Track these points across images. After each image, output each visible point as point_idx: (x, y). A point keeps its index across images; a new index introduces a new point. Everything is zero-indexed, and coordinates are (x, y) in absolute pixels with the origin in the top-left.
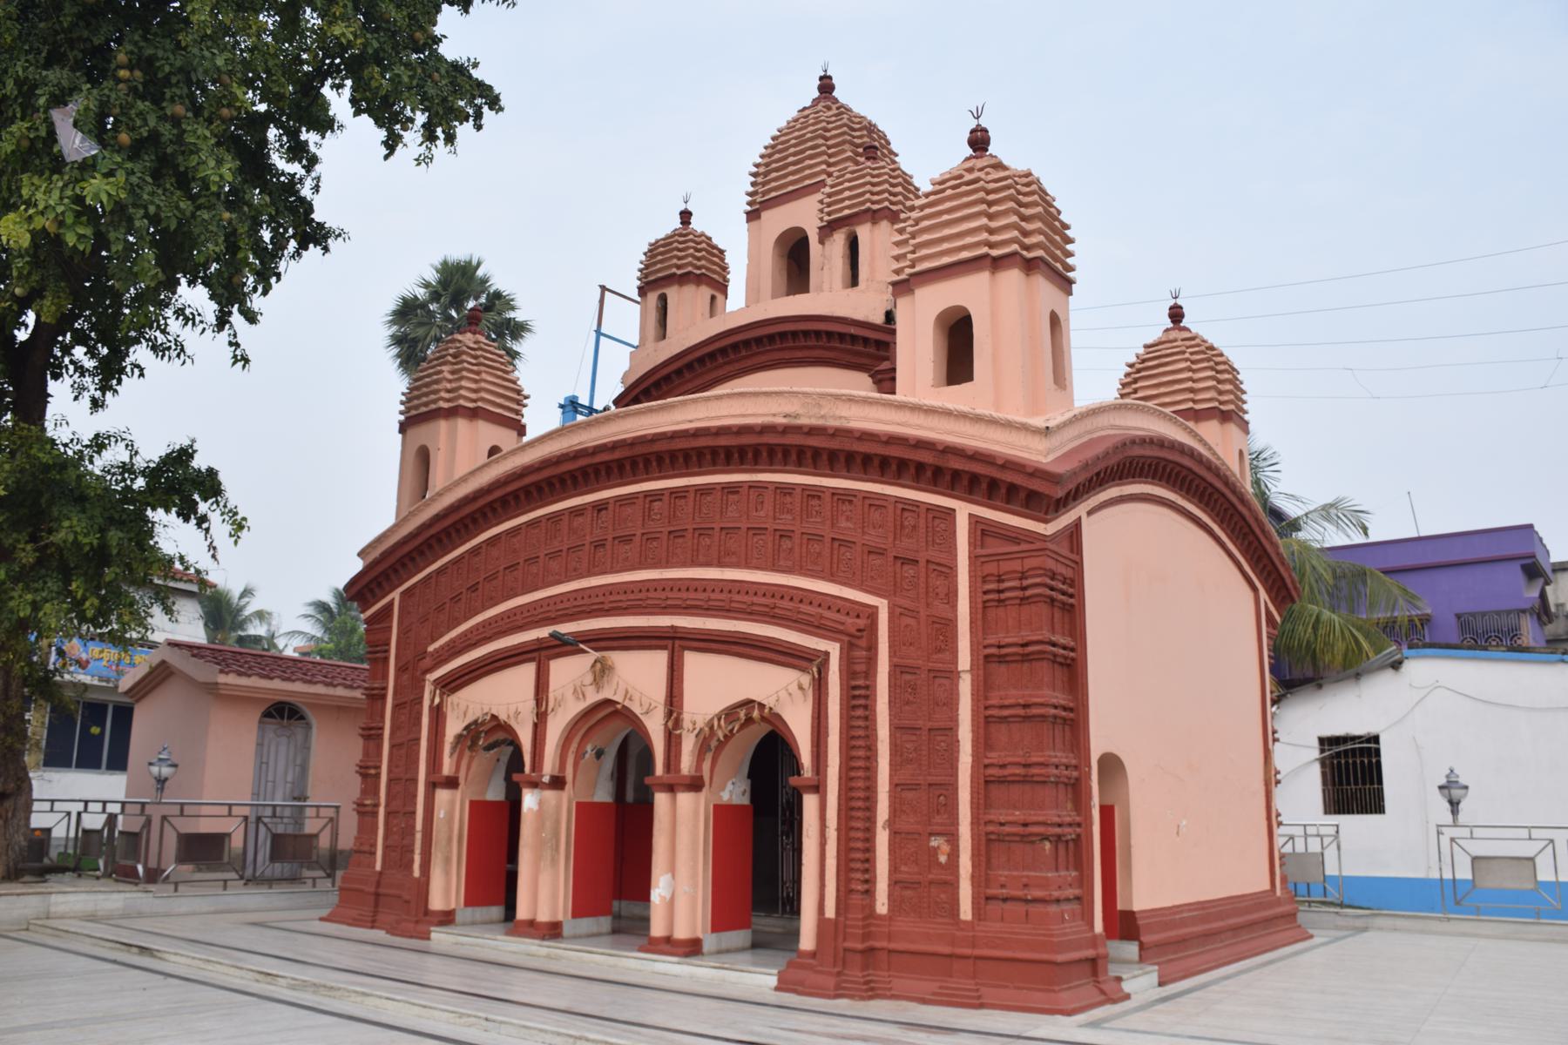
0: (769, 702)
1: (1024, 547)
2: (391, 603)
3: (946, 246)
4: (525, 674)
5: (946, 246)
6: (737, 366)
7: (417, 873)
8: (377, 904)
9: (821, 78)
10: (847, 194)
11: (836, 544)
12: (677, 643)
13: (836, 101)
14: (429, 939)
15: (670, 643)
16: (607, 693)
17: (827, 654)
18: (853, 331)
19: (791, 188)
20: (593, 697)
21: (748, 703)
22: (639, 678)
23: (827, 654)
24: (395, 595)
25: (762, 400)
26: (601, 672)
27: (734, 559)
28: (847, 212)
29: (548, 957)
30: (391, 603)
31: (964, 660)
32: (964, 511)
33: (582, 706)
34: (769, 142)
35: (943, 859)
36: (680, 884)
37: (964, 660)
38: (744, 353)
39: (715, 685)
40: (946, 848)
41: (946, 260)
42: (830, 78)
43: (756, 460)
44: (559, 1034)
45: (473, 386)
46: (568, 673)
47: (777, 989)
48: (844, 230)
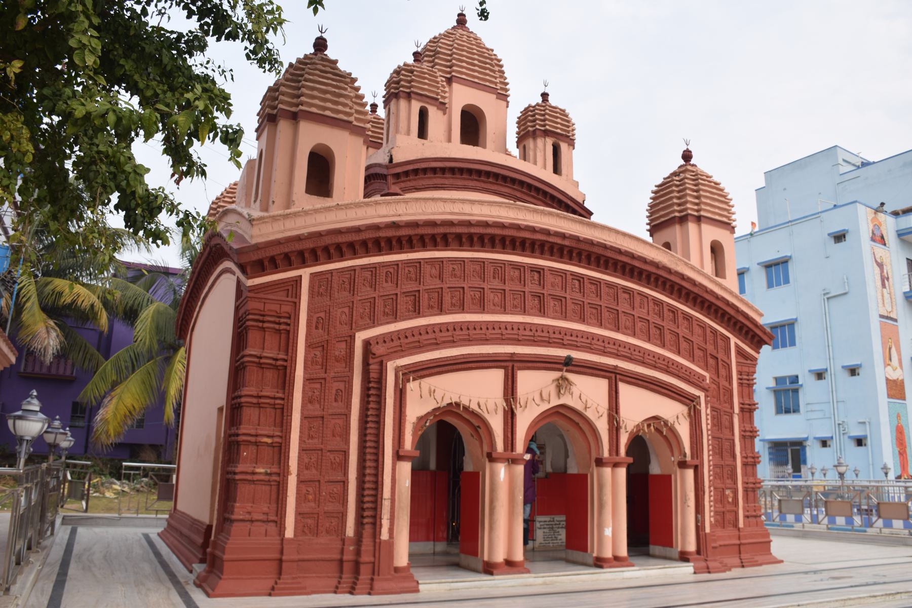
0: (671, 421)
1: (749, 362)
2: (298, 280)
3: (717, 211)
4: (496, 376)
5: (717, 211)
6: (483, 185)
7: (385, 536)
8: (280, 573)
9: (459, 15)
10: (559, 120)
11: (394, 297)
12: (618, 376)
13: (467, 30)
14: (417, 591)
15: (613, 375)
16: (563, 401)
17: (699, 397)
18: (569, 202)
19: (476, 80)
20: (555, 402)
21: (656, 418)
22: (589, 394)
23: (699, 397)
24: (305, 273)
25: (643, 245)
26: (562, 385)
27: (629, 332)
28: (559, 131)
29: (545, 584)
30: (737, 346)
31: (737, 409)
32: (733, 340)
33: (545, 407)
34: (437, 35)
35: (730, 500)
36: (504, 524)
37: (737, 409)
38: (490, 180)
39: (638, 406)
40: (731, 495)
41: (717, 217)
42: (464, 15)
43: (461, 244)
44: (837, 601)
45: (696, 207)
46: (531, 383)
47: (695, 573)
48: (554, 139)
